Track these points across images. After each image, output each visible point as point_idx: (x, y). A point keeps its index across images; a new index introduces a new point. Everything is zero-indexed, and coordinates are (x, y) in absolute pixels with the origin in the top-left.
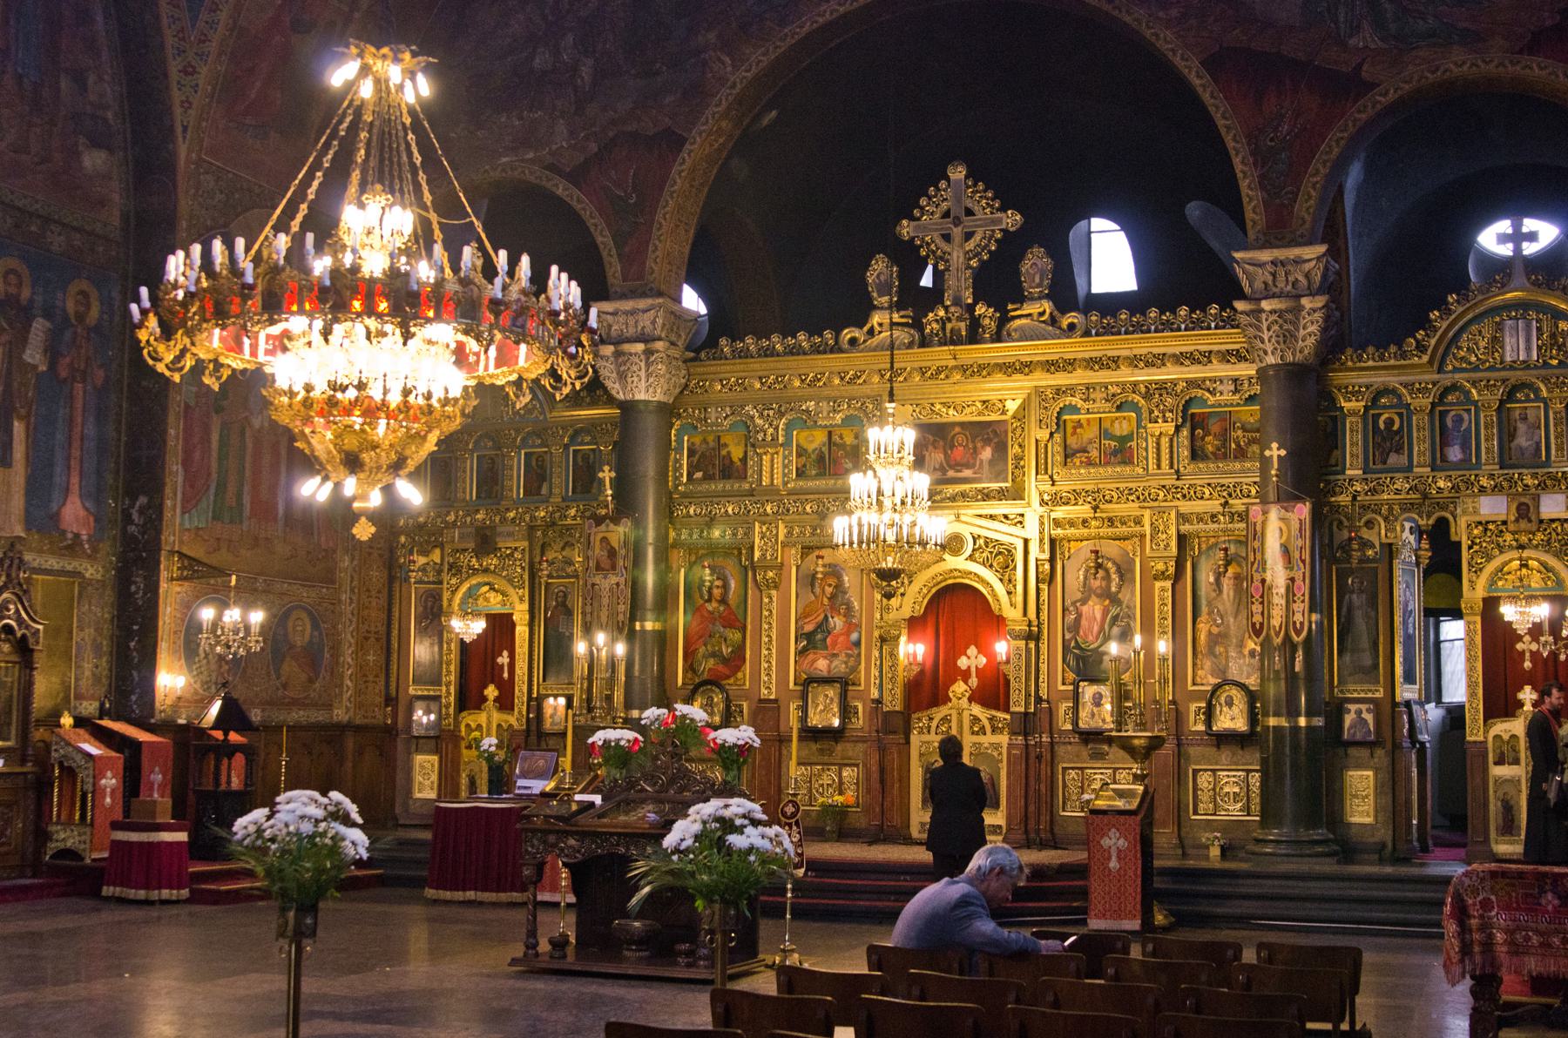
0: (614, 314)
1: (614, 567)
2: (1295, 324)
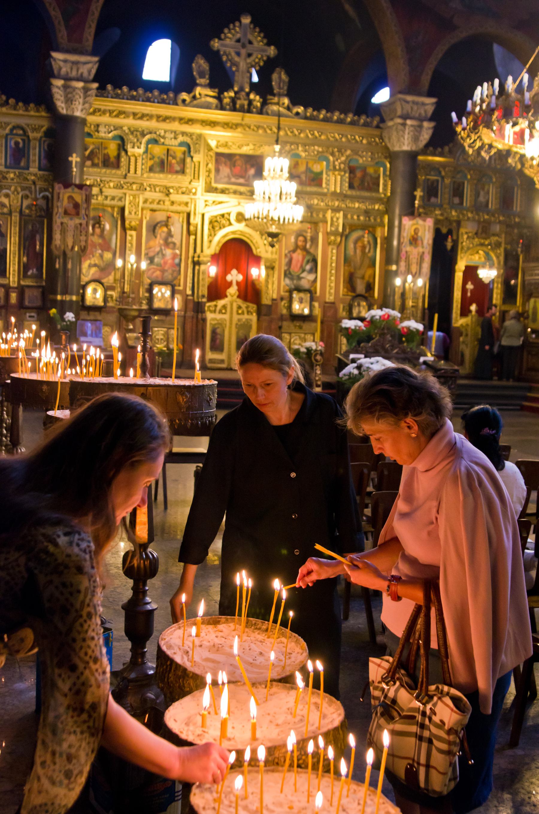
0: (65, 61)
1: (78, 214)
2: (420, 132)
